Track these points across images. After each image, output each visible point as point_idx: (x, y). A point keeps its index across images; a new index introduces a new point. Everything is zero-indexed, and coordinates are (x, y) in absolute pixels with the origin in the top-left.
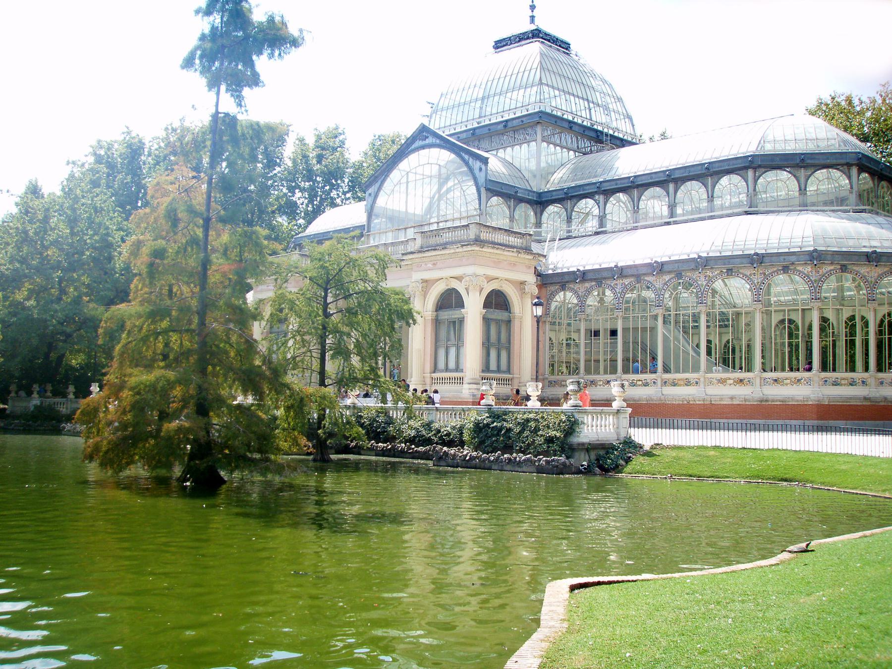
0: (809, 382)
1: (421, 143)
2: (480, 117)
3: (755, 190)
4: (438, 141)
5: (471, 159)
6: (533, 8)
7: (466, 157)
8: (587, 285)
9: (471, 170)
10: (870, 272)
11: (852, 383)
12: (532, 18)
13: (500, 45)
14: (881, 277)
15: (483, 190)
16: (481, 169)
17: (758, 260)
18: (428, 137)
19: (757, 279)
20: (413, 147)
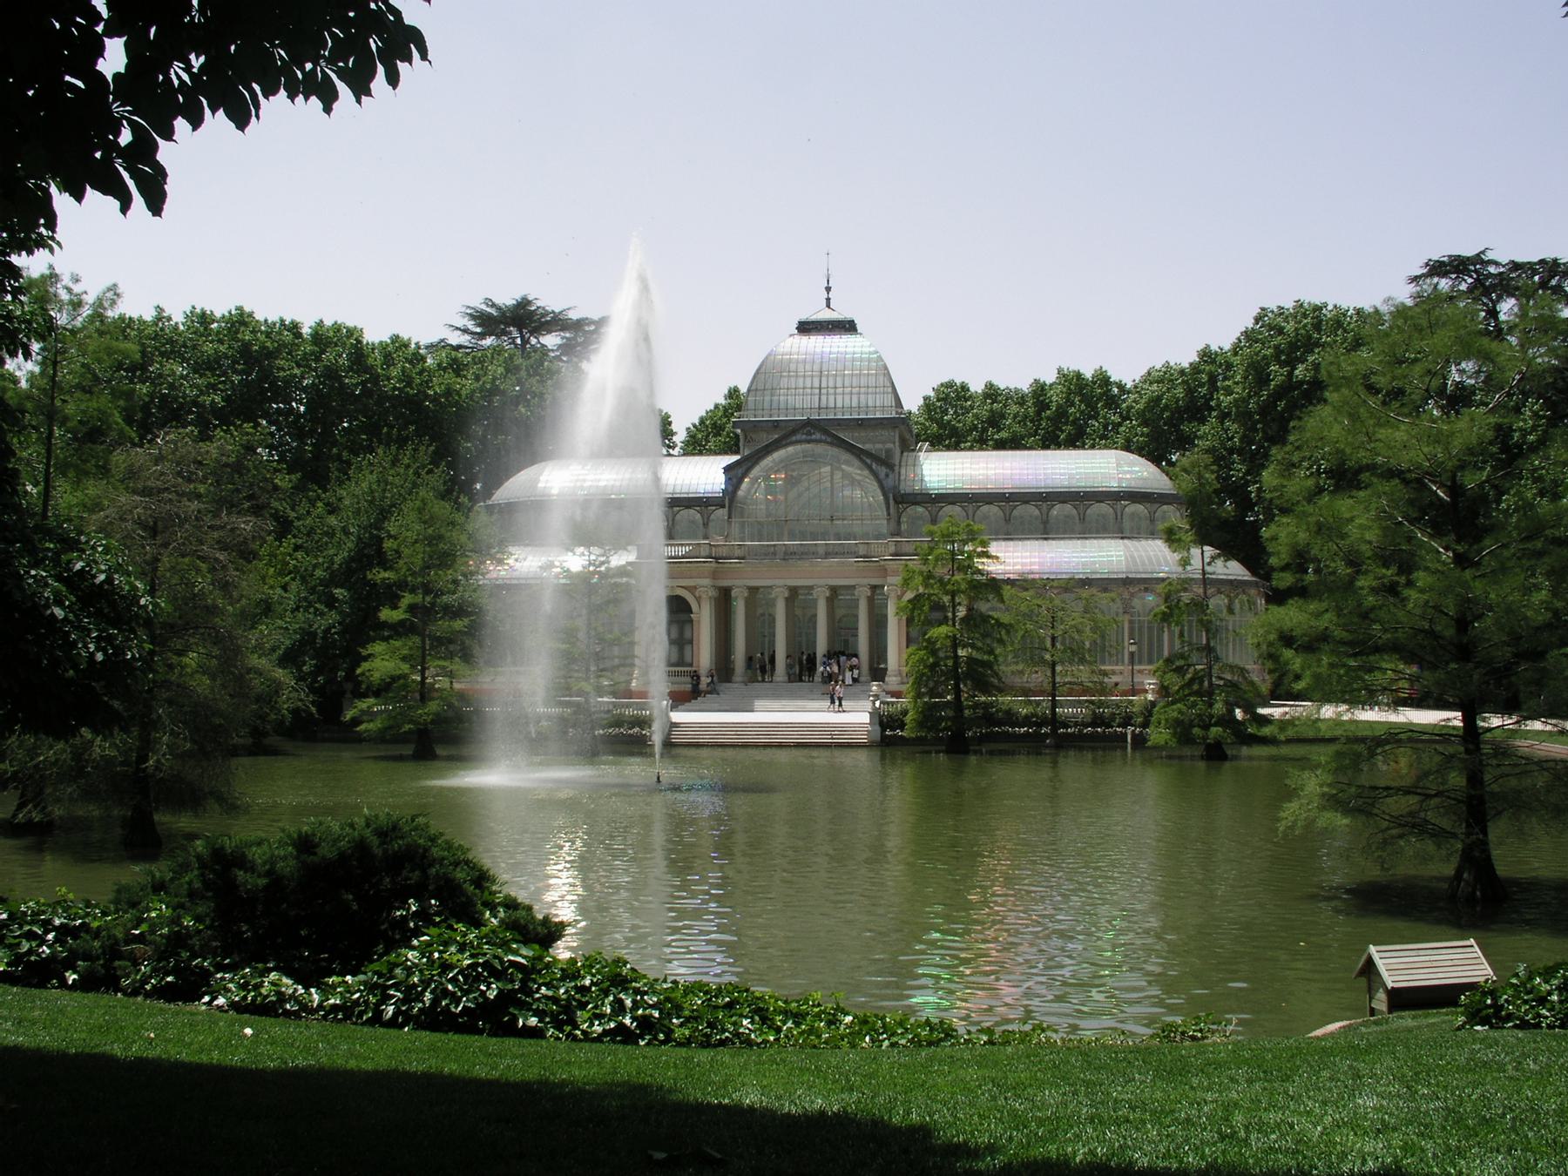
2: (819, 408)
4: (829, 440)
6: (828, 289)
7: (869, 461)
9: (875, 475)
12: (828, 300)
16: (887, 475)
20: (794, 438)
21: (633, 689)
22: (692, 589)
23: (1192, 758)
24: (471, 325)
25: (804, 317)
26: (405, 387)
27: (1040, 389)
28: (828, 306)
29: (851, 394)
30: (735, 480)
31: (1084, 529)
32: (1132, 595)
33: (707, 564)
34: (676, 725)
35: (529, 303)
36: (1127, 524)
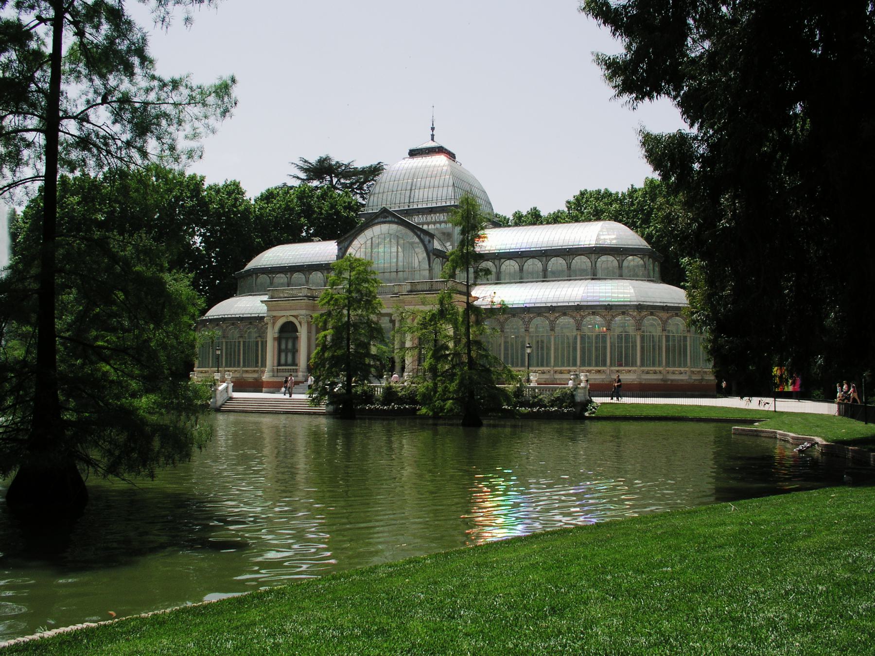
0: (635, 371)
1: (382, 220)
2: (409, 203)
3: (595, 266)
4: (396, 220)
5: (422, 234)
6: (433, 129)
7: (419, 233)
8: (506, 316)
9: (422, 241)
10: (664, 315)
11: (655, 372)
12: (433, 136)
13: (413, 153)
14: (668, 318)
15: (431, 254)
16: (429, 242)
17: (609, 308)
18: (388, 217)
19: (608, 318)
20: (376, 221)
21: (264, 380)
22: (296, 317)
23: (457, 425)
24: (303, 175)
25: (414, 147)
26: (219, 208)
27: (633, 191)
28: (433, 140)
29: (397, 191)
30: (343, 249)
31: (570, 275)
32: (583, 317)
33: (302, 301)
34: (231, 398)
35: (327, 159)
36: (625, 271)
